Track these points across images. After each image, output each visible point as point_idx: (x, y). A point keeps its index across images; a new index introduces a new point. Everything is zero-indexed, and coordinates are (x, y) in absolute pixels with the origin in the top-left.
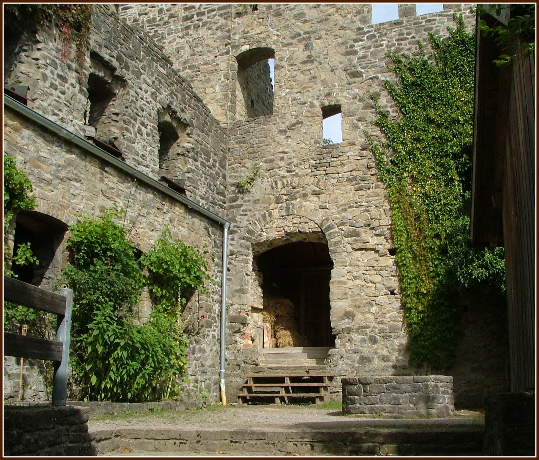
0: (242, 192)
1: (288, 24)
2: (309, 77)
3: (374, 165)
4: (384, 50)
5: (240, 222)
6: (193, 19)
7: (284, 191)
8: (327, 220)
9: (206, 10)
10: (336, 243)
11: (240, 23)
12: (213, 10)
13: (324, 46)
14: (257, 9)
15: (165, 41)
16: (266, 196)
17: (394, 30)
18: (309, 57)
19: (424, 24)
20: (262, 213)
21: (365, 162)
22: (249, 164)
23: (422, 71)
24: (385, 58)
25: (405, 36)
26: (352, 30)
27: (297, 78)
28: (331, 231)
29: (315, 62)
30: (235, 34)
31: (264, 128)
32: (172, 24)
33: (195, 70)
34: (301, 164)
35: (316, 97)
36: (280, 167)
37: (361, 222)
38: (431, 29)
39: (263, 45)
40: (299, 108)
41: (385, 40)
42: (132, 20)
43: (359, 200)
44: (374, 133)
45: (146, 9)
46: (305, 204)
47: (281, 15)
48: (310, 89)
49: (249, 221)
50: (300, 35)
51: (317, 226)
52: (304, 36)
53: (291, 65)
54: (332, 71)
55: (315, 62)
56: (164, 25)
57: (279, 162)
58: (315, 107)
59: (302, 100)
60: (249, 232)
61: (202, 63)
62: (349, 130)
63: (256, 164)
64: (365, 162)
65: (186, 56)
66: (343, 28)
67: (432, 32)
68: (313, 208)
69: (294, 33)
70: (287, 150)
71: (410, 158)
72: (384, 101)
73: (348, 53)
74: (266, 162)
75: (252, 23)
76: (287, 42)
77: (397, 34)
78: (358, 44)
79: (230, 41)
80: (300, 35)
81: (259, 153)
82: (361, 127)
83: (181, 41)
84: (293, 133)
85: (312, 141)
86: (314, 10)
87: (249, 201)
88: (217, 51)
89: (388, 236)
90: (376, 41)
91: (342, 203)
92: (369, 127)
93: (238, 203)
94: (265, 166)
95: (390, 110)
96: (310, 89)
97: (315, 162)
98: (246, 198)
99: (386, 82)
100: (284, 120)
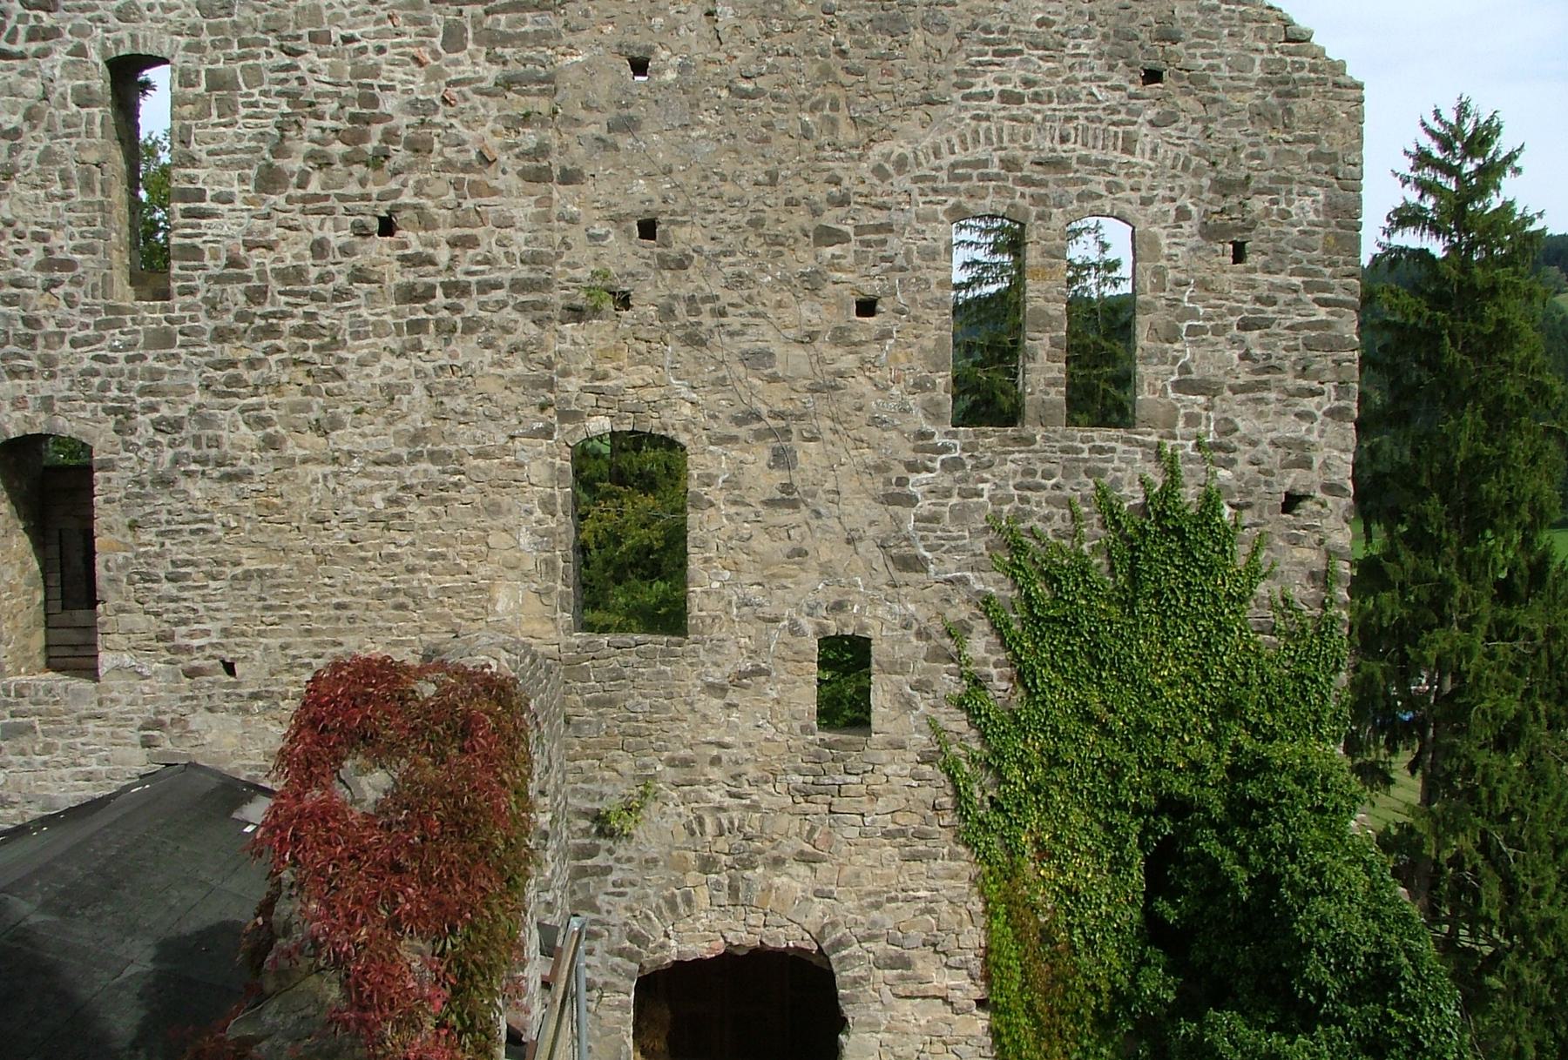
0: (611, 835)
1: (724, 378)
2: (787, 546)
3: (947, 801)
4: (983, 507)
5: (609, 912)
6: (432, 302)
7: (722, 844)
8: (834, 924)
9: (473, 279)
10: (856, 982)
11: (581, 340)
12: (497, 286)
13: (825, 463)
14: (628, 307)
15: (343, 354)
16: (675, 853)
17: (1011, 457)
18: (787, 488)
19: (1086, 455)
20: (666, 893)
21: (927, 793)
22: (626, 765)
23: (1077, 585)
24: (986, 530)
25: (1038, 479)
26: (903, 433)
27: (754, 544)
28: (844, 953)
29: (802, 507)
30: (565, 373)
31: (665, 672)
32: (362, 301)
33: (451, 467)
34: (766, 782)
35: (805, 608)
36: (709, 782)
37: (917, 935)
38: (1101, 473)
39: (652, 425)
40: (759, 631)
41: (985, 481)
42: (224, 261)
43: (911, 885)
44: (953, 726)
45: (268, 231)
46: (777, 881)
47: (703, 343)
48: (788, 582)
49: (632, 910)
50: (759, 418)
51: (807, 936)
52: (772, 423)
53: (735, 503)
54: (850, 541)
55: (802, 507)
56: (335, 299)
57: (708, 769)
58: (804, 634)
59: (768, 611)
60: (635, 937)
61: (471, 448)
62: (892, 709)
63: (645, 767)
64: (927, 793)
65: (417, 416)
66: (875, 421)
67: (1105, 481)
68: (800, 894)
69: (743, 407)
70: (727, 739)
71: (1038, 801)
72: (980, 645)
73: (890, 499)
74: (671, 762)
75: (616, 349)
76: (725, 432)
77: (1020, 469)
78: (920, 476)
79: (552, 396)
80: (759, 418)
81: (653, 738)
82: (922, 707)
83: (400, 364)
84: (744, 695)
85: (796, 725)
86: (798, 351)
87: (630, 860)
88: (514, 421)
89: (978, 972)
90: (965, 480)
91: (870, 888)
92: (942, 710)
93: (600, 860)
94: (671, 773)
95: (994, 672)
96: (788, 582)
97: (801, 779)
98: (621, 852)
99: (988, 600)
100: (718, 658)
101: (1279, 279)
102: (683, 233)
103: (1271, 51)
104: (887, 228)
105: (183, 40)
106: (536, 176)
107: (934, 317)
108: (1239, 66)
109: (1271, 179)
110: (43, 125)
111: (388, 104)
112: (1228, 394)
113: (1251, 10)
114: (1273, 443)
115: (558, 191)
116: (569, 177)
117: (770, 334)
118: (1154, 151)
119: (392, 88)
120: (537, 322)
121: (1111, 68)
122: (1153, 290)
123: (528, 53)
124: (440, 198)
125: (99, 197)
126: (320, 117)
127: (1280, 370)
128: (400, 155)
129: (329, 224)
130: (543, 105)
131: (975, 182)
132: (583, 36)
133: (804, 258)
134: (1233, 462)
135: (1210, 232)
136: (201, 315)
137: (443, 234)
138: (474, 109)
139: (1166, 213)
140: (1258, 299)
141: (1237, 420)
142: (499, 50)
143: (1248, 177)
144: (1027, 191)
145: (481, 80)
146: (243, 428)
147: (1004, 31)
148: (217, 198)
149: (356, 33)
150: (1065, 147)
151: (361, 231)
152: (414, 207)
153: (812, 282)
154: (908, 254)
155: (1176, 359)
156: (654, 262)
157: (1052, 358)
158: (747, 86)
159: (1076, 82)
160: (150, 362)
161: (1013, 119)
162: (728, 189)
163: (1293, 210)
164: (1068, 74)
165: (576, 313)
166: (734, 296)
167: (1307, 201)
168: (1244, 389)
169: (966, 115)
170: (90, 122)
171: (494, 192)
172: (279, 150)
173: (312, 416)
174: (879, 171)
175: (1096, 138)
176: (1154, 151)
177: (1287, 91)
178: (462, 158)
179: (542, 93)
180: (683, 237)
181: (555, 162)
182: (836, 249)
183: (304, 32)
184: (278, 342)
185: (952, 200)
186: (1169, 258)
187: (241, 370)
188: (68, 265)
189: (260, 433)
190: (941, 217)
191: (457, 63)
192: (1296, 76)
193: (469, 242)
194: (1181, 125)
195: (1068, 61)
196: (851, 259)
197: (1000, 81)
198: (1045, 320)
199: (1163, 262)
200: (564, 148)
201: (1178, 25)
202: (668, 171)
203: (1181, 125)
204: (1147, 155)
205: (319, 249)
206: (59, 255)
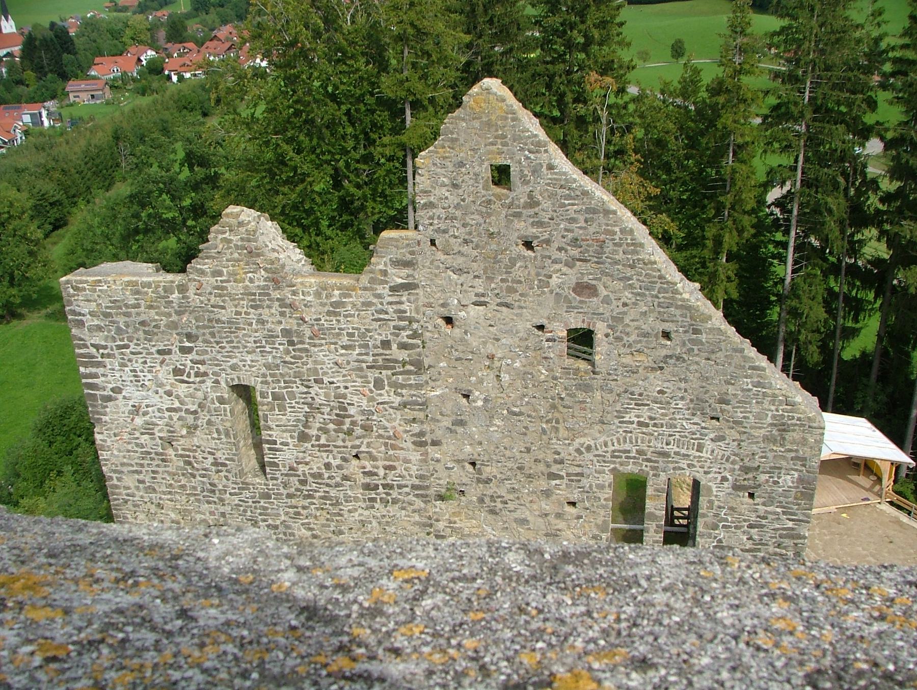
15: (342, 507)
30: (438, 520)
45: (305, 458)
47: (496, 514)
83: (366, 513)
86: (540, 520)
101: (769, 509)
102: (488, 469)
103: (777, 410)
104: (582, 475)
105: (260, 380)
106: (422, 444)
107: (602, 512)
108: (760, 416)
109: (771, 468)
110: (206, 410)
111: (352, 411)
115: (430, 449)
116: (435, 443)
117: (528, 513)
118: (713, 451)
119: (353, 405)
120: (425, 502)
121: (694, 415)
122: (708, 508)
123: (413, 392)
124: (379, 450)
125: (233, 440)
126: (323, 414)
127: (767, 545)
128: (358, 431)
129: (331, 456)
130: (421, 415)
132: (438, 383)
133: (543, 484)
135: (737, 487)
136: (281, 488)
137: (380, 463)
138: (390, 414)
140: (758, 517)
142: (399, 390)
145: (393, 402)
146: (303, 530)
147: (641, 395)
148: (282, 444)
149: (335, 380)
151: (344, 460)
152: (367, 452)
153: (547, 493)
154: (591, 486)
155: (715, 537)
156: (475, 480)
158: (516, 410)
159: (675, 419)
160: (262, 504)
161: (643, 433)
162: (508, 453)
163: (780, 481)
164: (671, 416)
165: (441, 498)
166: (511, 497)
167: (789, 477)
169: (621, 430)
170: (225, 410)
171: (402, 449)
172: (306, 426)
173: (332, 529)
174: (578, 451)
175: (683, 445)
176: (713, 451)
177: (783, 428)
178: (386, 434)
179: (420, 410)
180: (488, 471)
181: (428, 438)
182: (557, 482)
183: (312, 378)
184: (314, 501)
185: (612, 466)
186: (716, 496)
187: (300, 510)
188: (224, 465)
189: (310, 533)
191: (381, 395)
192: (789, 422)
193: (391, 468)
194: (727, 442)
196: (564, 486)
198: (654, 517)
199: (713, 498)
200: (432, 431)
201: (729, 398)
202: (480, 443)
203: (727, 442)
205: (328, 466)
206: (219, 461)
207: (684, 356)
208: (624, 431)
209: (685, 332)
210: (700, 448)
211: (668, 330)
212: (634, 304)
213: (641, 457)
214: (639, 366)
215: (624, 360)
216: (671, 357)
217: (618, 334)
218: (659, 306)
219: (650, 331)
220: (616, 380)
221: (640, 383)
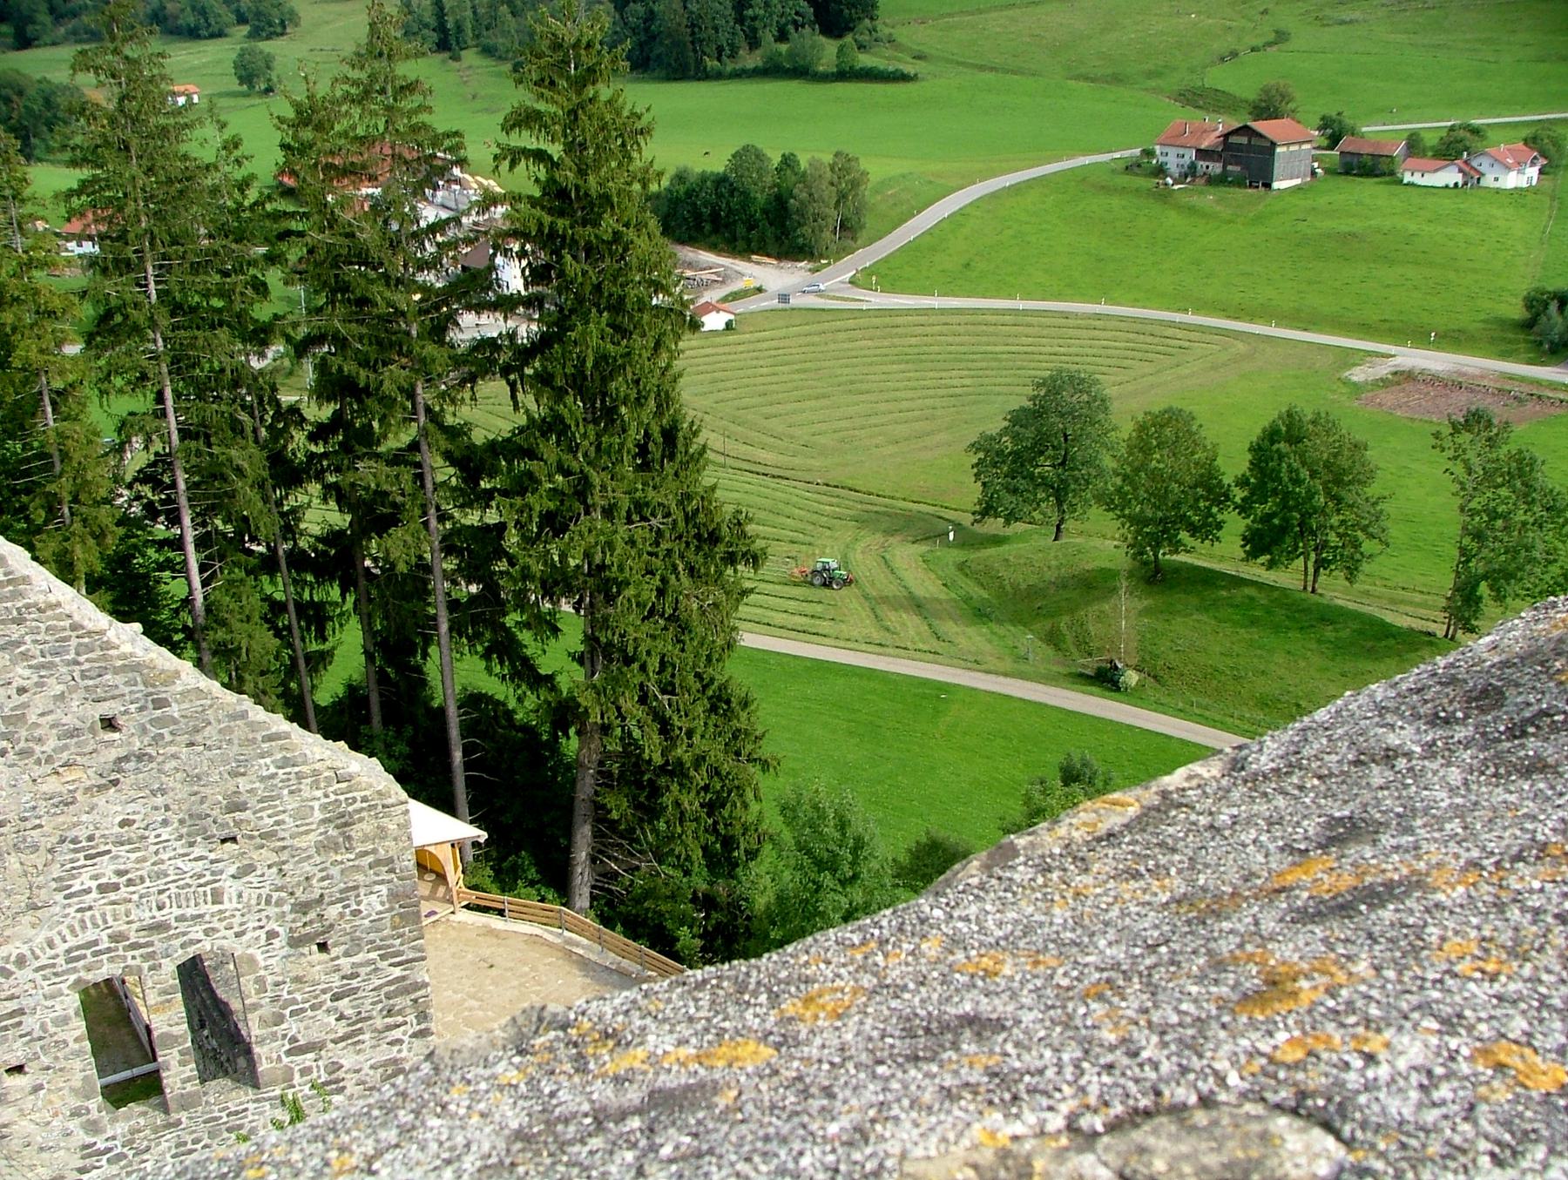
25: (190, 1146)
38: (240, 1127)
101: (355, 959)
103: (326, 796)
104: (21, 1012)
107: (77, 1064)
108: (301, 814)
109: (341, 892)
112: (331, 1046)
113: (304, 769)
114: (372, 1067)
118: (240, 896)
121: (191, 844)
122: (258, 992)
127: (370, 1018)
131: (90, 959)
134: (344, 1088)
135: (295, 942)
139: (257, 939)
140: (343, 978)
141: (342, 1061)
143: (322, 895)
144: (136, 953)
147: (90, 838)
150: (164, 912)
154: (43, 1027)
157: (182, 1063)
159: (162, 862)
161: (114, 903)
163: (362, 907)
164: (155, 859)
167: (374, 897)
168: (342, 1039)
169: (71, 910)
175: (188, 900)
176: (240, 896)
177: (344, 822)
185: (73, 978)
186: (266, 968)
190: (66, 992)
192: (350, 809)
194: (259, 872)
195: (153, 848)
197: (95, 877)
198: (170, 1040)
199: (262, 973)
203: (259, 872)
204: (235, 899)
207: (149, 750)
208: (78, 911)
209: (141, 709)
210: (217, 897)
211: (110, 714)
212: (37, 685)
213: (120, 946)
214: (75, 791)
215: (44, 788)
216: (126, 759)
217: (22, 744)
218: (84, 676)
219: (79, 724)
220: (40, 826)
221: (84, 818)
